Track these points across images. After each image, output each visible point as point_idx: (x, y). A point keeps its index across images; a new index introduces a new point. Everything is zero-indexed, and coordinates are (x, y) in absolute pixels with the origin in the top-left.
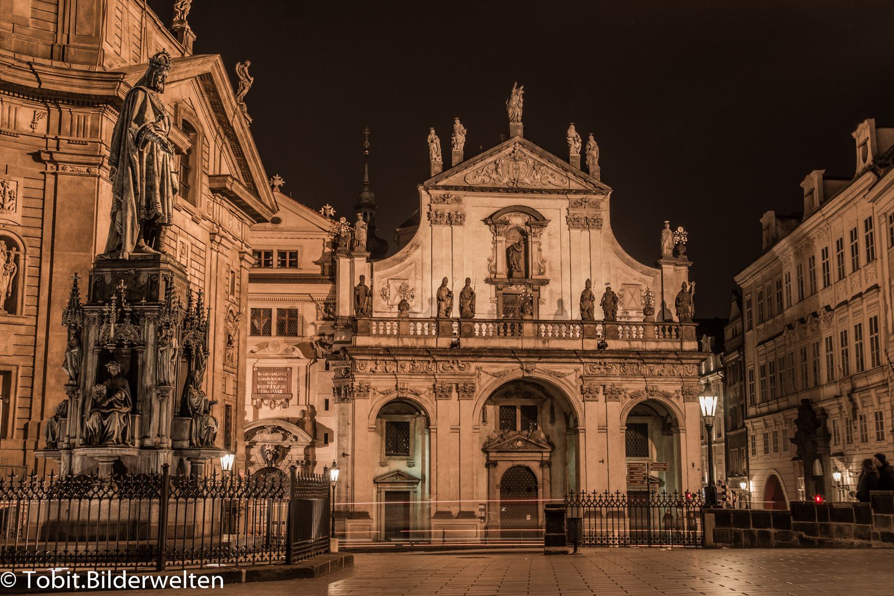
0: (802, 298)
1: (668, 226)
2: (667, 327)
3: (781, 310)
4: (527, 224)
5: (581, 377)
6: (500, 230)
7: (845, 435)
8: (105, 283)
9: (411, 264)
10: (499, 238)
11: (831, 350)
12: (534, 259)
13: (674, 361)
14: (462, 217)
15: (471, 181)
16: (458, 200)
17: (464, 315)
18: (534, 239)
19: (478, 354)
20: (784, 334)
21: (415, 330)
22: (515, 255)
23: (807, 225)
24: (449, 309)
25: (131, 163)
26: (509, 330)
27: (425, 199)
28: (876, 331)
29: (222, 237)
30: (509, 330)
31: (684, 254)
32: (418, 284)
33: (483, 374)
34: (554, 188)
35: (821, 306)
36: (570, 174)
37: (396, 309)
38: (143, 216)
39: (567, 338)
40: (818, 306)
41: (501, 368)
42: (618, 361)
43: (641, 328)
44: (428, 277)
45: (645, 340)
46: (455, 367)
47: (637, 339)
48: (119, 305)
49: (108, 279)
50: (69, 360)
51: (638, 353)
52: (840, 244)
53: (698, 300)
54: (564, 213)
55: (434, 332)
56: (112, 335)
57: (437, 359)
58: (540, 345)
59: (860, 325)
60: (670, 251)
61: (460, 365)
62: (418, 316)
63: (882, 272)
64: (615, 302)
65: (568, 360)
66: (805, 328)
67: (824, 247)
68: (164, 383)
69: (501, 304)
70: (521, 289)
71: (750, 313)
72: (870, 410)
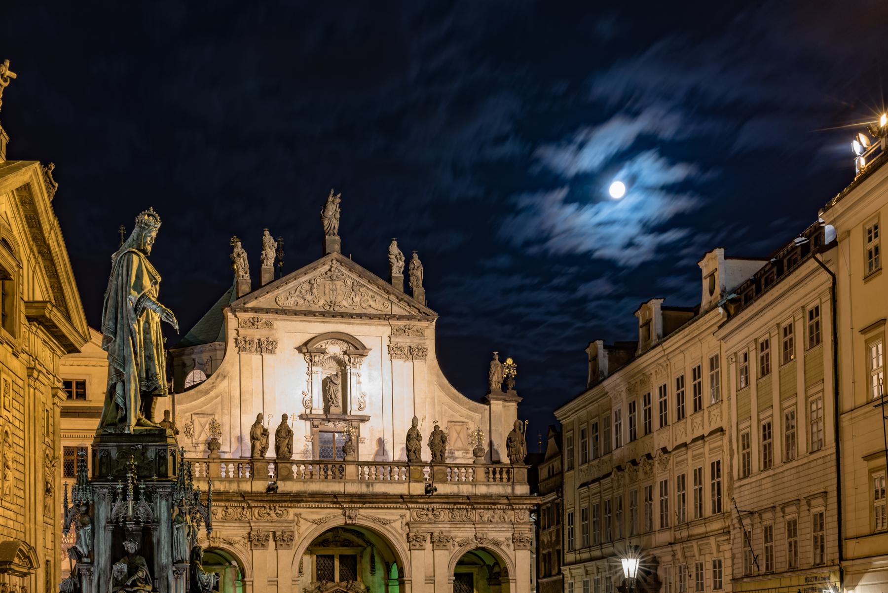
0: (633, 437)
1: (497, 357)
2: (498, 470)
3: (608, 451)
4: (345, 353)
5: (407, 524)
6: (318, 358)
7: (678, 584)
8: (111, 458)
9: (217, 397)
10: (314, 369)
11: (666, 494)
12: (354, 392)
13: (505, 507)
14: (274, 343)
15: (284, 303)
16: (269, 325)
17: (281, 456)
18: (353, 370)
19: (297, 498)
20: (612, 476)
21: (227, 472)
22: (333, 388)
23: (645, 361)
24: (264, 450)
25: (131, 333)
26: (330, 472)
27: (232, 323)
28: (719, 476)
29: (40, 371)
30: (330, 472)
31: (513, 389)
32: (226, 419)
33: (302, 521)
34: (374, 312)
35: (656, 448)
36: (392, 297)
37: (202, 447)
38: (144, 388)
39: (392, 481)
40: (653, 448)
41: (322, 514)
42: (447, 506)
43: (470, 470)
44: (236, 411)
45: (474, 483)
46: (272, 513)
47: (466, 483)
48: (133, 483)
49: (114, 454)
50: (83, 538)
51: (468, 497)
52: (680, 382)
53: (531, 438)
54: (386, 341)
55: (248, 474)
56: (130, 512)
57: (253, 504)
58: (363, 489)
59: (700, 469)
60: (499, 385)
61: (278, 511)
62: (226, 456)
63: (729, 414)
64: (443, 442)
65: (394, 505)
66: (637, 471)
67: (662, 384)
68: (182, 561)
69: (317, 442)
70: (341, 426)
71: (571, 452)
72: (708, 558)
